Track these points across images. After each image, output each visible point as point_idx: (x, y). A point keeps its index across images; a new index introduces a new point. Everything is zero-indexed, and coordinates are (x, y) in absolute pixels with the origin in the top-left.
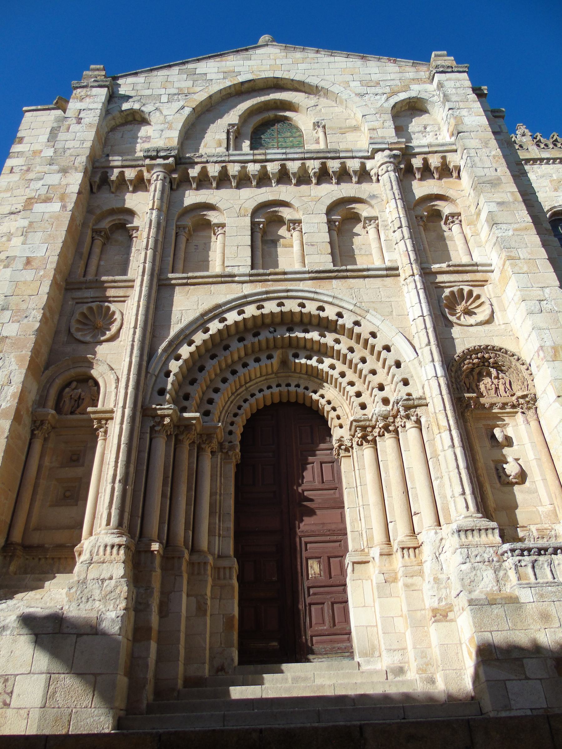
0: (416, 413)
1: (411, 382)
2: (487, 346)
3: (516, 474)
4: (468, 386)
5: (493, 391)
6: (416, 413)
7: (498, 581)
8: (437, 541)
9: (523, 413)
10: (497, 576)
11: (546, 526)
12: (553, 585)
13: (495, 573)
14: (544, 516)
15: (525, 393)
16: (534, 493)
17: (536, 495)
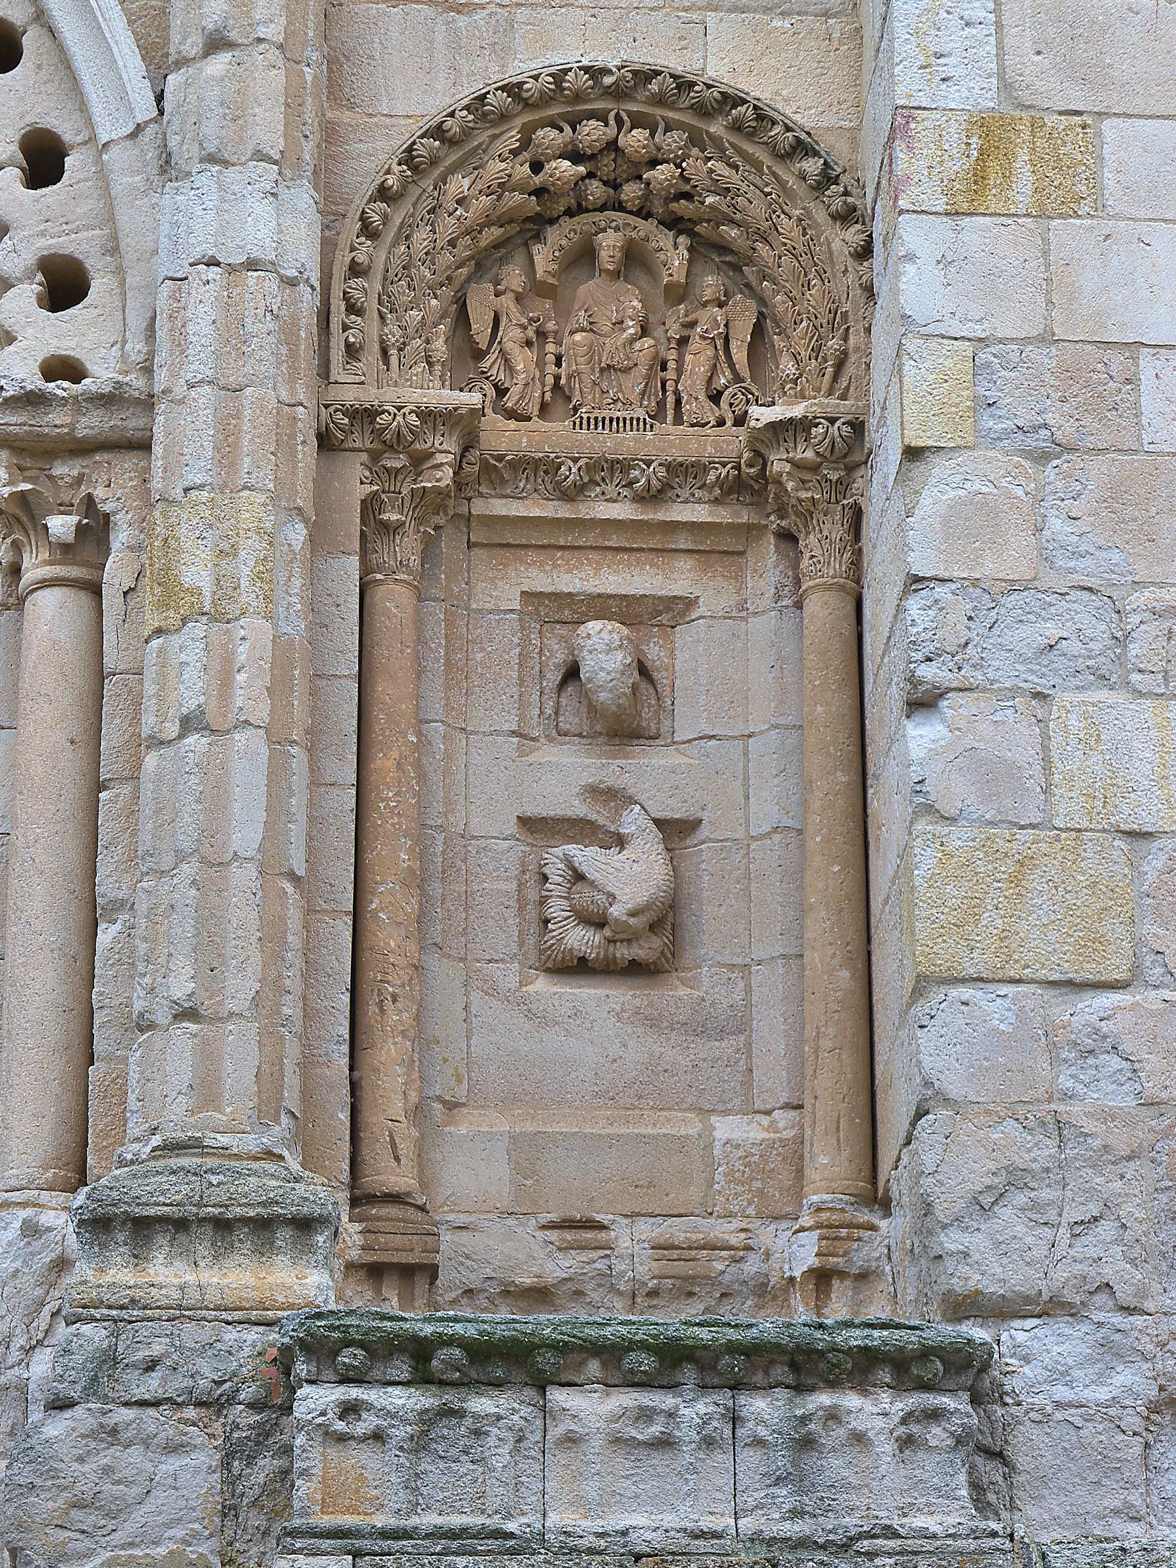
0: (84, 490)
1: (98, 287)
2: (645, 76)
3: (633, 914)
4: (480, 327)
5: (633, 385)
6: (84, 490)
7: (228, 1511)
8: (27, 1281)
9: (788, 537)
10: (231, 1482)
11: (725, 1230)
12: (493, 1544)
13: (226, 1465)
14: (729, 1174)
15: (797, 411)
16: (721, 1033)
17: (729, 1045)
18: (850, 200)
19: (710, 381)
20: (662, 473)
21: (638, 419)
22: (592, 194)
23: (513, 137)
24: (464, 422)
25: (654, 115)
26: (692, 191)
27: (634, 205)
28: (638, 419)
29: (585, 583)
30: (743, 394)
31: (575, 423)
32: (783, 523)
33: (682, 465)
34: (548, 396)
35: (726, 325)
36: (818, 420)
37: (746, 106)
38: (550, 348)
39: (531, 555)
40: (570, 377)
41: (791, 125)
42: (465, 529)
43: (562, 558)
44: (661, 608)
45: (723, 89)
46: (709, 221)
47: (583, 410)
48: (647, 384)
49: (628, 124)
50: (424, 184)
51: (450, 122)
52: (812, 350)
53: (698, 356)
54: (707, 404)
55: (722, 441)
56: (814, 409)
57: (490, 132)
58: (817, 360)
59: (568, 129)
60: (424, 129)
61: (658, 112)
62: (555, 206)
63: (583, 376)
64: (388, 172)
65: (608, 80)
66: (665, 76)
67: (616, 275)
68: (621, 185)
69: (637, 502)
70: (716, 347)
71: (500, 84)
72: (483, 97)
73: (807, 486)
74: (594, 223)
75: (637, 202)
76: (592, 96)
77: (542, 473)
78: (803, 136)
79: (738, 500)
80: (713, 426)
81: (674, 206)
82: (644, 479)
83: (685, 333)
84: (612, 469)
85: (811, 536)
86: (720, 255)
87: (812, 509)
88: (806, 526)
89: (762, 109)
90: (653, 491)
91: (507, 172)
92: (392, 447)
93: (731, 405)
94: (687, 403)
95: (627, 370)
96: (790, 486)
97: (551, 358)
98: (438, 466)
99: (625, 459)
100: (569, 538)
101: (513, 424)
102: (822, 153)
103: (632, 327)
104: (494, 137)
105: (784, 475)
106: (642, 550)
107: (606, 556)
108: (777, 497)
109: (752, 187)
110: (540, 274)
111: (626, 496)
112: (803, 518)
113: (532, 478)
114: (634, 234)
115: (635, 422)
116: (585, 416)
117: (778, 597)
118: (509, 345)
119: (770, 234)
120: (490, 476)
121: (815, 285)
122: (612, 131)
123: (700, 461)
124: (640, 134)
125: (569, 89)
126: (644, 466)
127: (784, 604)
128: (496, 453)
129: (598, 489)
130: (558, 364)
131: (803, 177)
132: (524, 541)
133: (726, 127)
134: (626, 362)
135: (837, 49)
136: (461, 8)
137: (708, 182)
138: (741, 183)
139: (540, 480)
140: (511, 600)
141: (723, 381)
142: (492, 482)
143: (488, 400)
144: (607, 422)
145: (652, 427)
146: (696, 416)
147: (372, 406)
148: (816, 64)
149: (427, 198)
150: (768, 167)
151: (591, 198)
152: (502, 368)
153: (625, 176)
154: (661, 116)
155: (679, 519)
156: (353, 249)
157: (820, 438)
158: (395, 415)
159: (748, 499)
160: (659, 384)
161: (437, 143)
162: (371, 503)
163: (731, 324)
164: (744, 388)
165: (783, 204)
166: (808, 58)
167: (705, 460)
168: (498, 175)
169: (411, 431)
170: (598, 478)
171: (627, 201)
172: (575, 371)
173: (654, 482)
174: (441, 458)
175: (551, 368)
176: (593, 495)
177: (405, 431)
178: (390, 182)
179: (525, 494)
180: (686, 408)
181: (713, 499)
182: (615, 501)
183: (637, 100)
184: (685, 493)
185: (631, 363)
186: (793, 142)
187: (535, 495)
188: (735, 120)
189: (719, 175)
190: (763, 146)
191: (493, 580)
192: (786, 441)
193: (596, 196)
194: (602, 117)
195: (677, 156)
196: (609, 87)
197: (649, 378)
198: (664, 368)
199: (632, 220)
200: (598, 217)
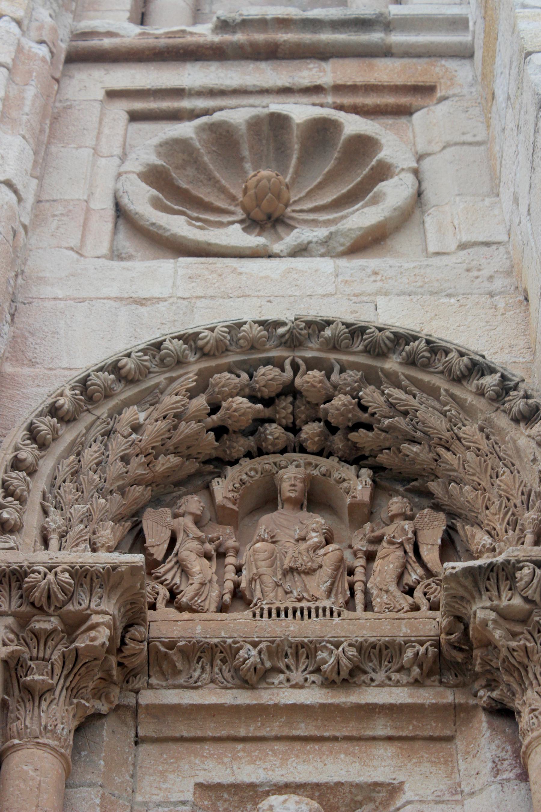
18: (530, 401)
19: (400, 577)
20: (352, 652)
21: (324, 610)
22: (271, 434)
23: (189, 378)
24: (125, 584)
25: (329, 359)
26: (371, 419)
27: (314, 443)
28: (324, 610)
29: (270, 773)
30: (437, 584)
31: (254, 615)
32: (495, 694)
33: (374, 647)
34: (227, 598)
35: (415, 533)
36: (521, 564)
37: (417, 342)
38: (230, 560)
39: (208, 748)
40: (252, 581)
41: (464, 350)
42: (132, 723)
43: (243, 750)
44: (359, 798)
45: (394, 330)
46: (389, 449)
47: (264, 602)
48: (333, 584)
49: (303, 367)
50: (98, 412)
51: (125, 360)
52: (508, 523)
53: (386, 559)
54: (398, 594)
55: (418, 622)
56: (516, 553)
57: (167, 375)
58: (514, 531)
59: (245, 376)
60: (100, 365)
61: (332, 356)
62: (235, 444)
63: (265, 578)
64: (61, 395)
65: (281, 330)
66: (338, 324)
67: (297, 504)
68: (300, 430)
69: (327, 687)
70: (405, 552)
71: (177, 334)
72: (161, 343)
73: (518, 638)
74: (275, 464)
75: (316, 439)
76: (267, 347)
77: (219, 662)
78: (478, 358)
79: (441, 682)
80: (407, 611)
81: (353, 436)
82: (333, 659)
83: (372, 548)
84: (297, 655)
85: (529, 692)
86: (404, 486)
87: (526, 661)
88: (521, 683)
89: (434, 342)
90: (344, 674)
91: (183, 403)
92: (41, 609)
93: (425, 594)
94: (377, 596)
95: (310, 572)
96: (498, 634)
97: (231, 568)
98: (93, 627)
99: (311, 642)
100: (252, 729)
101: (186, 615)
102: (498, 368)
103: (316, 536)
104: (171, 380)
105: (490, 623)
106: (335, 739)
107: (293, 748)
108: (485, 662)
109: (430, 409)
110: (219, 498)
111: (314, 682)
112: (516, 674)
113: (208, 668)
114: (316, 472)
115: (321, 611)
116: (266, 607)
117: (496, 771)
118: (184, 554)
119: (452, 443)
120: (161, 667)
121: (504, 473)
122: (289, 373)
123: (395, 641)
124: (316, 374)
125: (244, 337)
126: (332, 647)
127: (504, 777)
128: (167, 640)
129: (282, 677)
130: (239, 570)
131: (481, 393)
132: (199, 734)
133: (401, 363)
134: (310, 564)
135: (503, 314)
136: (144, 302)
137: (386, 409)
138: (419, 405)
139: (216, 670)
140: (183, 792)
141: (414, 577)
142: (163, 674)
143: (160, 598)
144: (290, 612)
145: (339, 615)
146: (388, 606)
147: (21, 567)
148: (484, 324)
149: (102, 423)
150: (446, 391)
151: (270, 437)
152: (178, 575)
153: (303, 416)
154: (335, 359)
155: (375, 701)
156: (17, 449)
157: (526, 579)
158: (45, 575)
159: (452, 680)
160: (347, 586)
161: (112, 376)
162: (16, 669)
163: (419, 533)
164: (438, 580)
165: (463, 420)
166: (477, 320)
167: (401, 640)
168: (174, 406)
169: (63, 590)
170: (281, 665)
171: (306, 440)
172: (255, 574)
173: (344, 661)
174: (95, 619)
175: (230, 575)
176: (276, 682)
177: (55, 588)
178: (61, 401)
179: (199, 684)
180: (376, 601)
181: (411, 680)
182: (302, 687)
183: (311, 349)
184: (380, 676)
185: (315, 566)
186: (470, 365)
187: (212, 685)
188: (409, 354)
189: (396, 399)
190: (439, 375)
191: (162, 774)
192: (488, 590)
193: (277, 435)
194: (279, 364)
195: (353, 389)
196: (283, 336)
197: (335, 578)
198: (351, 572)
199: (312, 459)
200: (278, 458)
